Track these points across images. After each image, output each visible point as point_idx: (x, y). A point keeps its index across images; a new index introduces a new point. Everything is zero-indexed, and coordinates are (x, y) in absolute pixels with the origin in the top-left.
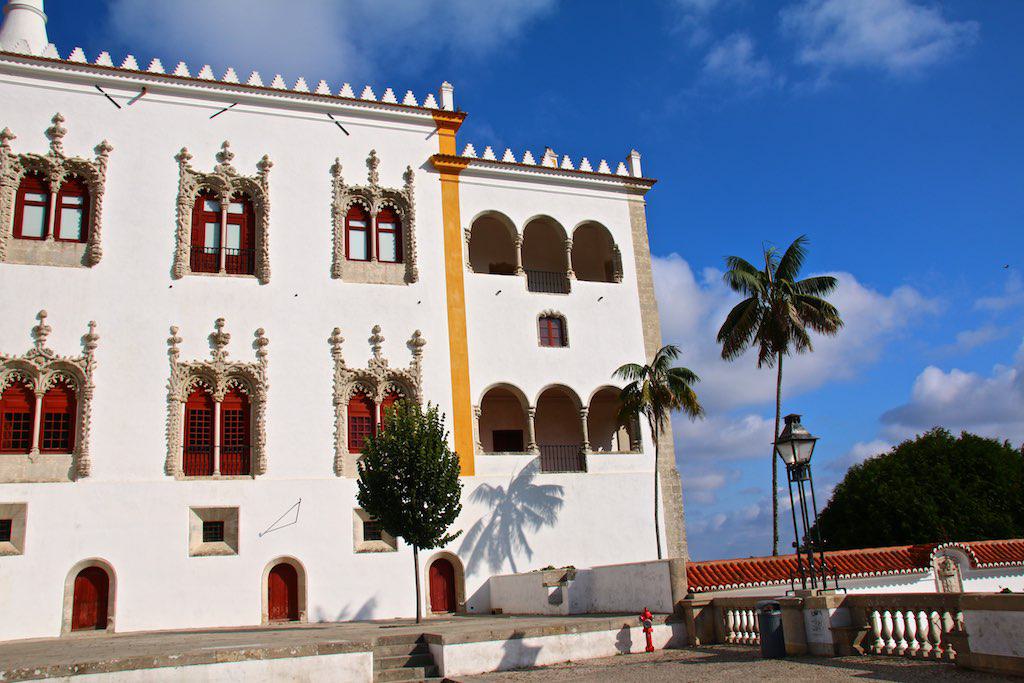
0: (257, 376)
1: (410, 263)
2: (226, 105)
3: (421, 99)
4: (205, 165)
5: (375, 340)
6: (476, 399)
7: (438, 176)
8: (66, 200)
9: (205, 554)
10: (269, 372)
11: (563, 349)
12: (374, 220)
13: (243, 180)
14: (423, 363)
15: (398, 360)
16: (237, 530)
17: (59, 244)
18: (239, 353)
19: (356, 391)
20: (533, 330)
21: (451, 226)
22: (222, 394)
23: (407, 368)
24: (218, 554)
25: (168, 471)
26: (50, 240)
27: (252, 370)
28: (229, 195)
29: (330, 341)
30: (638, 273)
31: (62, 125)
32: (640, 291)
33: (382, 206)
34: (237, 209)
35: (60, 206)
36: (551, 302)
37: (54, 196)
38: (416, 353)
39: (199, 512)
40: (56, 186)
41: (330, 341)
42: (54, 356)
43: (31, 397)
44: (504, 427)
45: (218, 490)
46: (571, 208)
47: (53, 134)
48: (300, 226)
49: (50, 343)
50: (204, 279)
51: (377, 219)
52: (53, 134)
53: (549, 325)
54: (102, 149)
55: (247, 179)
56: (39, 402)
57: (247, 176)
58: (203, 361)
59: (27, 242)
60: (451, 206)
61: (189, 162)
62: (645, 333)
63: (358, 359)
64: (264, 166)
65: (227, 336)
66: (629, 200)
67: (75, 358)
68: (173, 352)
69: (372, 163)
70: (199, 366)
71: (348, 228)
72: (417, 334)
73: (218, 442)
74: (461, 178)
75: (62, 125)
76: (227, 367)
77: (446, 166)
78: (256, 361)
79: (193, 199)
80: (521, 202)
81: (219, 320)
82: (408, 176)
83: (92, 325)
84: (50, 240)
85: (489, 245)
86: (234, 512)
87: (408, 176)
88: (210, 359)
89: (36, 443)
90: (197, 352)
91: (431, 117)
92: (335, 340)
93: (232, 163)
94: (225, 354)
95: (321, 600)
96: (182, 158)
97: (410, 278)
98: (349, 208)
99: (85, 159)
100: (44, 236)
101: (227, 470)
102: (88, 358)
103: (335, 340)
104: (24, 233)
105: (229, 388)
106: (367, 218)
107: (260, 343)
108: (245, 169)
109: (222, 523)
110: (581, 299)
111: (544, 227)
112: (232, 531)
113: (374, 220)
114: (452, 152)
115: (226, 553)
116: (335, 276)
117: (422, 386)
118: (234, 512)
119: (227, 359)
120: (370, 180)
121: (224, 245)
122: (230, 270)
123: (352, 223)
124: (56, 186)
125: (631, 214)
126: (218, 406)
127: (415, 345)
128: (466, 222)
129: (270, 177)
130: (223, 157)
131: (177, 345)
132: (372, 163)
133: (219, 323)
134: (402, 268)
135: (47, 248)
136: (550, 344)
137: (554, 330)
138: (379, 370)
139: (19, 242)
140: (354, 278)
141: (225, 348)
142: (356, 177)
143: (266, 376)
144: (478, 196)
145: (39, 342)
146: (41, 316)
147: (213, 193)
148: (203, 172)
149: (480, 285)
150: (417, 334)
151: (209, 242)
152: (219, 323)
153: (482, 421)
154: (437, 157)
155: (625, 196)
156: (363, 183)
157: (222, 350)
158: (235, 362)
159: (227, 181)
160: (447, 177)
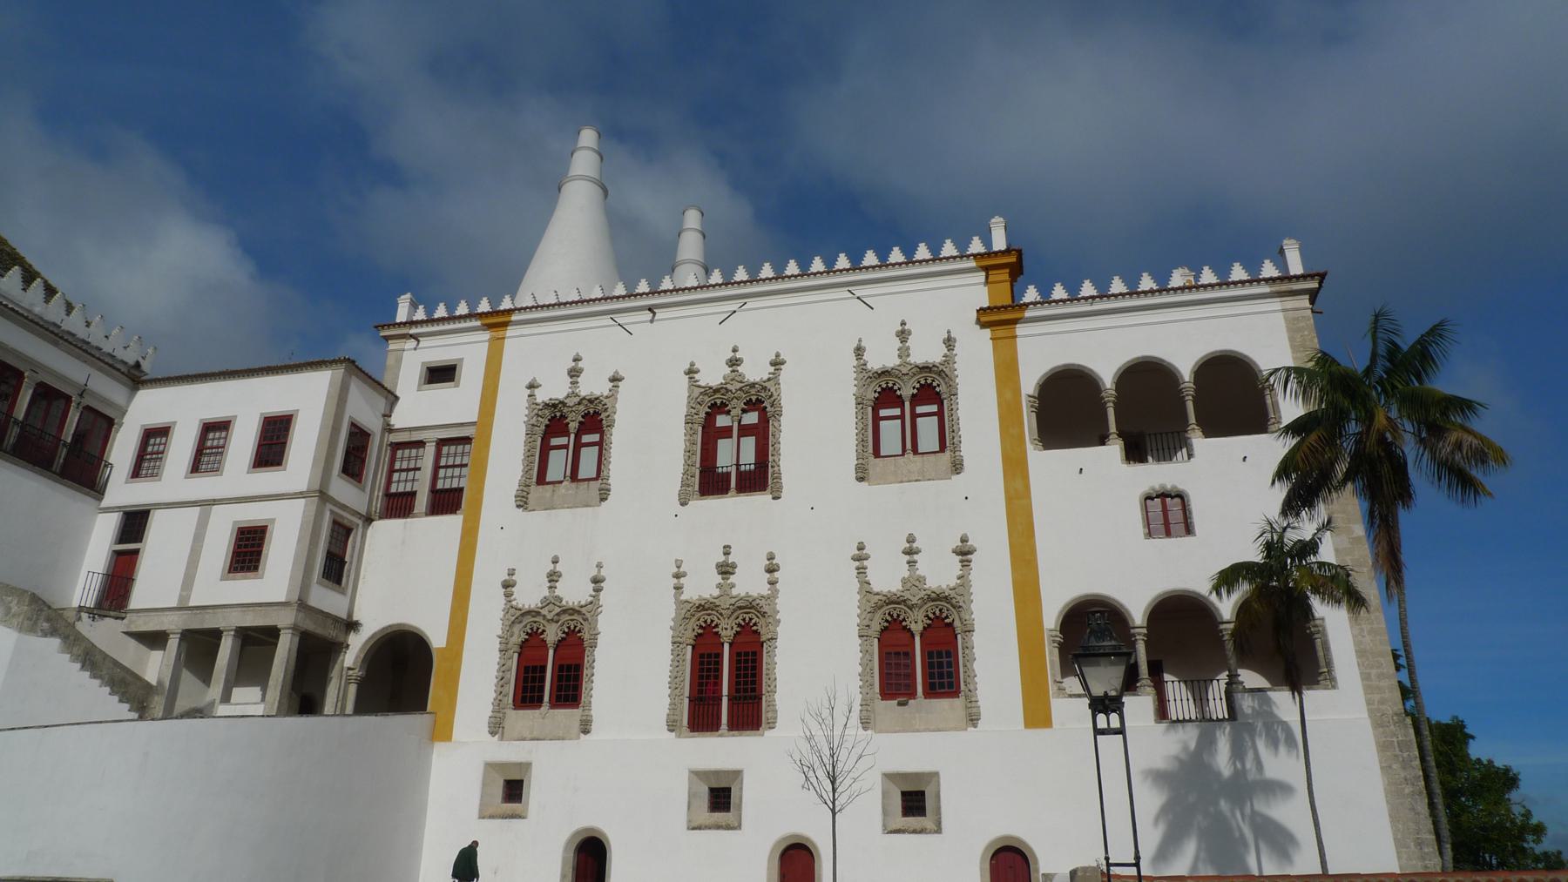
0: (766, 609)
2: (734, 305)
3: (962, 245)
4: (714, 375)
6: (1051, 619)
7: (987, 332)
8: (586, 439)
10: (781, 603)
12: (907, 405)
13: (753, 385)
15: (939, 573)
18: (748, 583)
21: (1009, 395)
23: (952, 585)
24: (718, 827)
25: (672, 726)
27: (762, 603)
31: (580, 364)
34: (752, 418)
36: (1156, 474)
38: (966, 564)
40: (573, 426)
45: (722, 750)
46: (1182, 338)
47: (574, 373)
48: (817, 426)
49: (561, 590)
50: (714, 503)
51: (906, 404)
52: (574, 373)
56: (551, 652)
60: (1007, 370)
61: (697, 376)
63: (888, 578)
64: (777, 363)
65: (734, 566)
68: (678, 588)
69: (903, 335)
71: (877, 419)
72: (964, 540)
73: (725, 691)
74: (1020, 330)
75: (580, 364)
77: (999, 319)
80: (1103, 344)
82: (949, 342)
83: (599, 566)
85: (1064, 409)
87: (949, 342)
90: (702, 586)
91: (972, 264)
92: (860, 557)
94: (733, 586)
96: (691, 372)
97: (957, 467)
99: (597, 393)
102: (594, 604)
103: (860, 557)
106: (899, 402)
108: (755, 371)
113: (907, 405)
114: (1008, 301)
115: (728, 827)
116: (861, 479)
118: (737, 774)
123: (883, 413)
124: (573, 426)
125: (1289, 330)
126: (726, 647)
127: (964, 552)
130: (734, 363)
131: (682, 580)
132: (903, 335)
133: (727, 550)
134: (946, 457)
137: (1169, 514)
140: (883, 480)
141: (732, 579)
142: (883, 356)
144: (1045, 348)
146: (555, 562)
147: (724, 405)
149: (1053, 469)
150: (964, 540)
152: (727, 550)
154: (981, 311)
155: (1276, 304)
156: (891, 361)
160: (1002, 332)
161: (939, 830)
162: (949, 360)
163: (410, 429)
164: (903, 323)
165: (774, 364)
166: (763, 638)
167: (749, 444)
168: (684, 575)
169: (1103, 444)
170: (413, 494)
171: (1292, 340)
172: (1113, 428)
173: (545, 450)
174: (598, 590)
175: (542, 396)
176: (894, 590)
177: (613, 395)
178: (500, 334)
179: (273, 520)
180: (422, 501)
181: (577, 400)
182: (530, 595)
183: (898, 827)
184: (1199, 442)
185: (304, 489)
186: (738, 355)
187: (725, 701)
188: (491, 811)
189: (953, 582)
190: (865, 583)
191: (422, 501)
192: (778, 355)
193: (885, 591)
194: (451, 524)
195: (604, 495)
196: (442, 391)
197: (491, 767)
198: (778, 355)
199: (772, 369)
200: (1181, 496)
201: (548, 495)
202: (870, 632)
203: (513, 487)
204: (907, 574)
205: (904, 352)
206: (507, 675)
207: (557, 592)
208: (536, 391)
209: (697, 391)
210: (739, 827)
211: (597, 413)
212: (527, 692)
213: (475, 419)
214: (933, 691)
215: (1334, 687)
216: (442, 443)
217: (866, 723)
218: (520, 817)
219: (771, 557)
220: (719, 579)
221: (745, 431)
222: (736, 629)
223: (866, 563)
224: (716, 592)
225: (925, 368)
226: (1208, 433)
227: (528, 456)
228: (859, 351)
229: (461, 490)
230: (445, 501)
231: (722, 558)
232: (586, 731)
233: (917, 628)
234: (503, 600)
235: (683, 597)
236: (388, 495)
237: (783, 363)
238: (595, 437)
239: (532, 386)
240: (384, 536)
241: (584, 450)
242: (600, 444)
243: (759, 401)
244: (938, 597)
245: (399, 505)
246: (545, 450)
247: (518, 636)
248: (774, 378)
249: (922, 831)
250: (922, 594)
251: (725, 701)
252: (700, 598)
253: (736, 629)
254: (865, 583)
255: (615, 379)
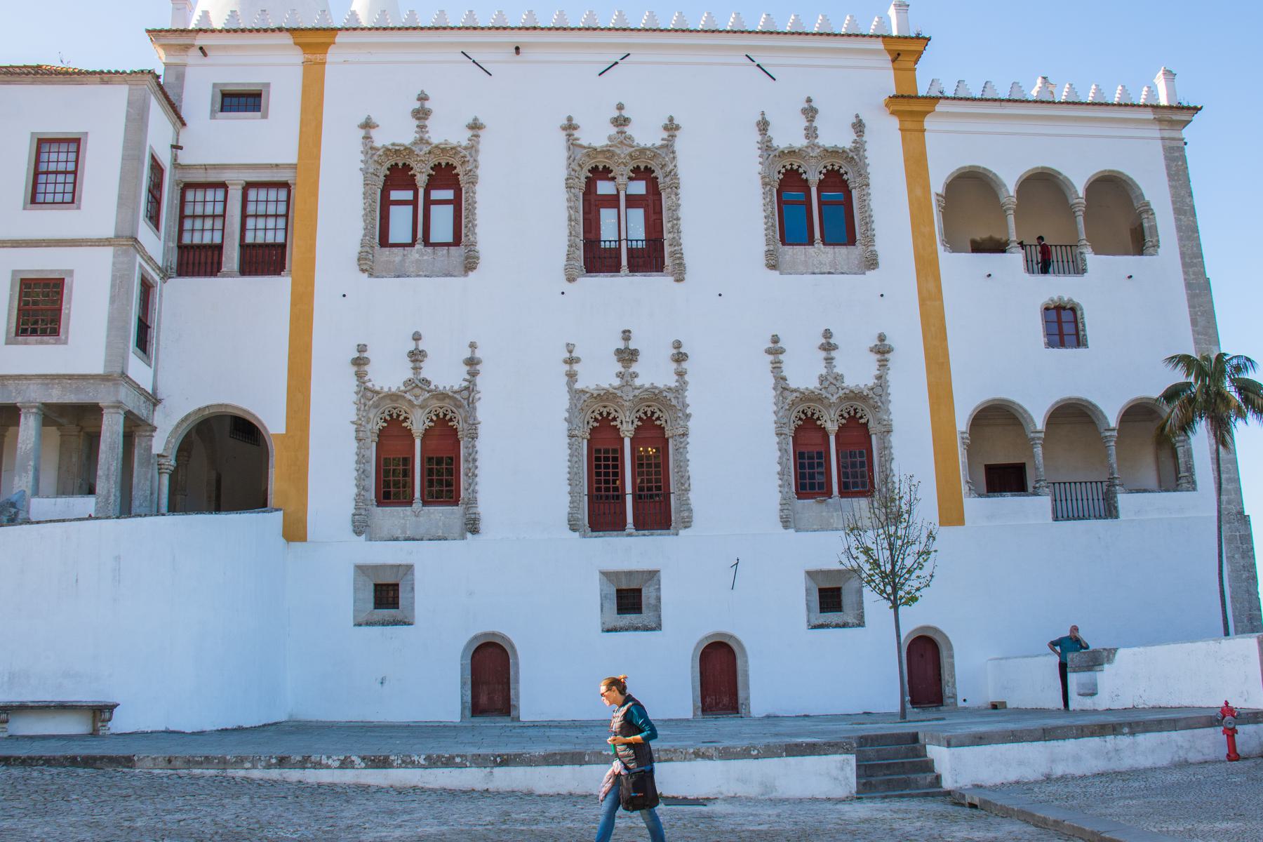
0: (674, 402)
1: (870, 240)
4: (597, 134)
5: (828, 347)
6: (962, 424)
8: (436, 195)
9: (621, 629)
10: (691, 396)
11: (1081, 351)
13: (643, 151)
14: (891, 377)
15: (857, 372)
16: (659, 599)
17: (429, 250)
18: (653, 373)
19: (803, 417)
20: (1036, 327)
21: (919, 192)
22: (632, 428)
24: (636, 629)
25: (573, 528)
26: (419, 246)
27: (670, 395)
28: (627, 171)
29: (769, 351)
30: (1181, 239)
32: (1184, 265)
33: (824, 171)
34: (639, 188)
35: (428, 203)
36: (1058, 287)
37: (421, 192)
38: (883, 364)
39: (607, 575)
40: (421, 180)
41: (769, 351)
42: (432, 387)
43: (409, 434)
44: (1002, 457)
45: (630, 551)
47: (421, 114)
52: (421, 114)
53: (1059, 316)
54: (475, 126)
55: (649, 149)
56: (418, 443)
57: (649, 145)
58: (606, 386)
59: (395, 250)
60: (916, 165)
61: (576, 134)
62: (1194, 322)
63: (805, 374)
64: (671, 127)
66: (1163, 139)
67: (456, 388)
68: (572, 376)
69: (810, 112)
70: (602, 393)
72: (882, 338)
73: (629, 489)
75: (428, 105)
76: (637, 392)
78: (672, 382)
79: (583, 180)
81: (624, 332)
82: (859, 126)
83: (473, 346)
84: (419, 246)
86: (652, 576)
87: (859, 126)
88: (617, 382)
89: (417, 494)
90: (600, 374)
92: (775, 350)
93: (629, 130)
94: (635, 375)
95: (764, 689)
96: (570, 127)
98: (781, 176)
100: (412, 245)
101: (641, 525)
102: (470, 389)
103: (775, 350)
104: (391, 241)
105: (640, 419)
107: (680, 358)
108: (646, 135)
109: (639, 591)
110: (1100, 285)
111: (1043, 185)
112: (653, 601)
115: (646, 629)
116: (773, 267)
117: (891, 407)
118: (653, 575)
119: (638, 382)
120: (807, 137)
121: (623, 236)
122: (634, 268)
124: (421, 180)
125: (1166, 158)
127: (882, 350)
128: (937, 185)
129: (679, 145)
130: (621, 122)
131: (576, 367)
132: (810, 112)
133: (626, 335)
135: (417, 256)
136: (1062, 344)
137: (1064, 326)
138: (832, 389)
139: (386, 250)
141: (635, 368)
142: (789, 135)
143: (688, 401)
145: (416, 369)
148: (594, 145)
150: (882, 338)
151: (608, 232)
152: (626, 335)
153: (971, 451)
155: (1155, 132)
156: (799, 141)
157: (631, 370)
158: (647, 385)
159: (623, 152)
160: (909, 125)
161: (861, 623)
162: (859, 147)
163: (206, 167)
164: (809, 100)
165: (666, 128)
166: (668, 434)
167: (637, 218)
168: (578, 360)
169: (1004, 251)
170: (219, 248)
171: (1168, 167)
172: (1013, 237)
173: (386, 204)
174: (474, 374)
175: (382, 139)
176: (811, 387)
177: (473, 148)
178: (319, 57)
179: (71, 272)
180: (232, 256)
181: (426, 149)
182: (389, 375)
183: (820, 622)
184: (1092, 259)
185: (111, 233)
186: (625, 113)
187: (629, 499)
188: (363, 617)
189: (871, 382)
190: (780, 380)
191: (232, 256)
192: (671, 119)
193: (802, 387)
194: (276, 289)
195: (470, 264)
196: (241, 124)
197: (362, 570)
198: (671, 119)
199: (665, 135)
200: (1073, 310)
201: (398, 259)
202: (786, 431)
203: (354, 247)
204: (824, 372)
205: (811, 132)
206: (367, 467)
207: (424, 374)
208: (373, 133)
209: (579, 154)
210: (658, 627)
211: (450, 167)
212: (390, 486)
213: (294, 160)
214: (845, 491)
215: (1194, 489)
216: (249, 186)
217: (786, 523)
218: (405, 623)
219: (678, 345)
220: (619, 367)
221: (633, 201)
222: (637, 423)
223: (781, 357)
224: (617, 382)
225: (835, 152)
226: (1097, 252)
227: (368, 214)
228: (763, 126)
229: (282, 247)
230: (264, 260)
231: (621, 345)
232: (474, 530)
233: (832, 427)
234: (354, 382)
235: (578, 386)
236: (182, 248)
237: (677, 128)
238: (448, 194)
239: (368, 125)
240: (182, 298)
241: (433, 208)
242: (457, 203)
243: (649, 170)
244: (856, 396)
245: (197, 261)
246: (386, 204)
247: (376, 424)
248: (668, 146)
249: (845, 625)
250: (841, 393)
251: (629, 499)
252: (598, 388)
253: (637, 423)
254: (780, 380)
255: (475, 126)
